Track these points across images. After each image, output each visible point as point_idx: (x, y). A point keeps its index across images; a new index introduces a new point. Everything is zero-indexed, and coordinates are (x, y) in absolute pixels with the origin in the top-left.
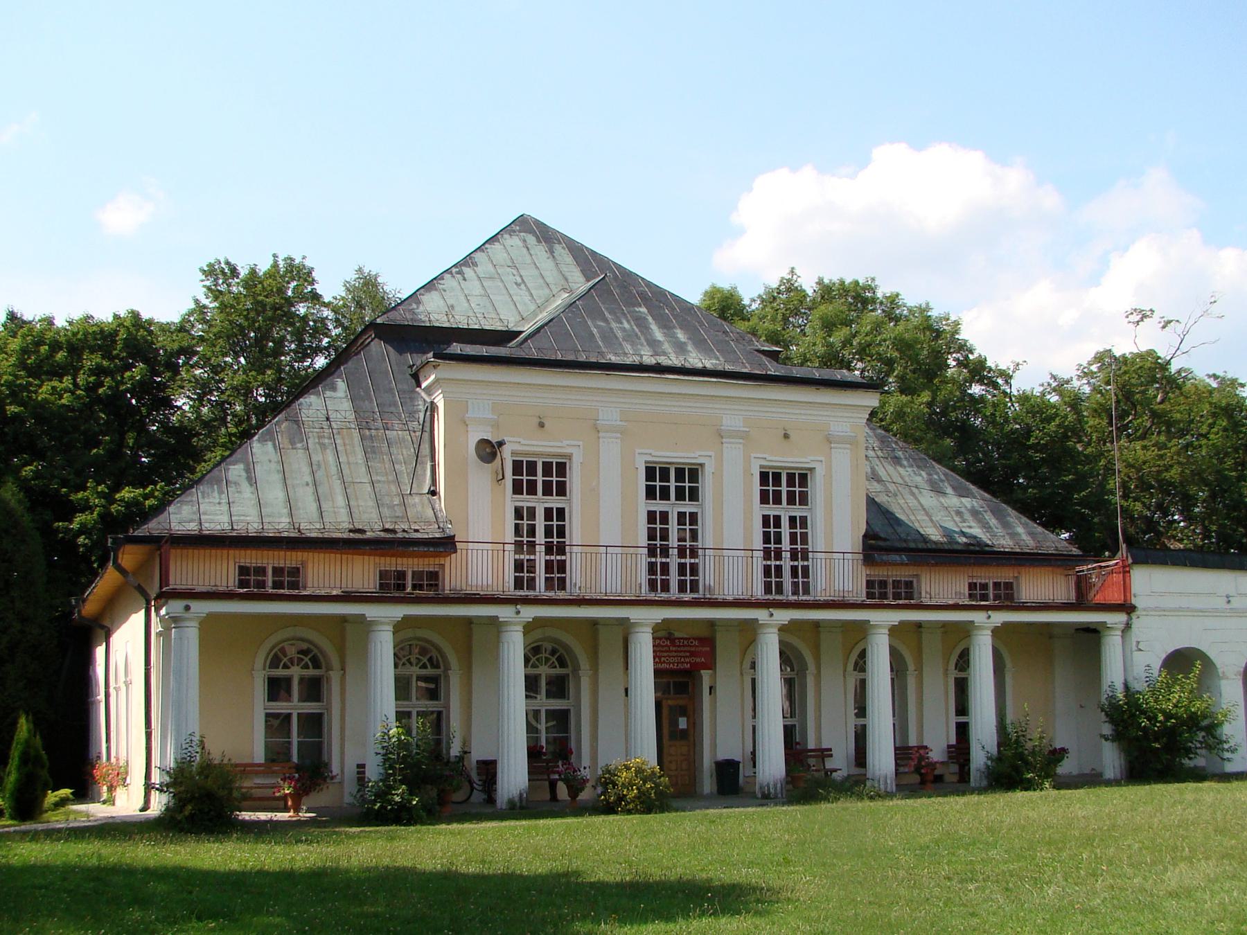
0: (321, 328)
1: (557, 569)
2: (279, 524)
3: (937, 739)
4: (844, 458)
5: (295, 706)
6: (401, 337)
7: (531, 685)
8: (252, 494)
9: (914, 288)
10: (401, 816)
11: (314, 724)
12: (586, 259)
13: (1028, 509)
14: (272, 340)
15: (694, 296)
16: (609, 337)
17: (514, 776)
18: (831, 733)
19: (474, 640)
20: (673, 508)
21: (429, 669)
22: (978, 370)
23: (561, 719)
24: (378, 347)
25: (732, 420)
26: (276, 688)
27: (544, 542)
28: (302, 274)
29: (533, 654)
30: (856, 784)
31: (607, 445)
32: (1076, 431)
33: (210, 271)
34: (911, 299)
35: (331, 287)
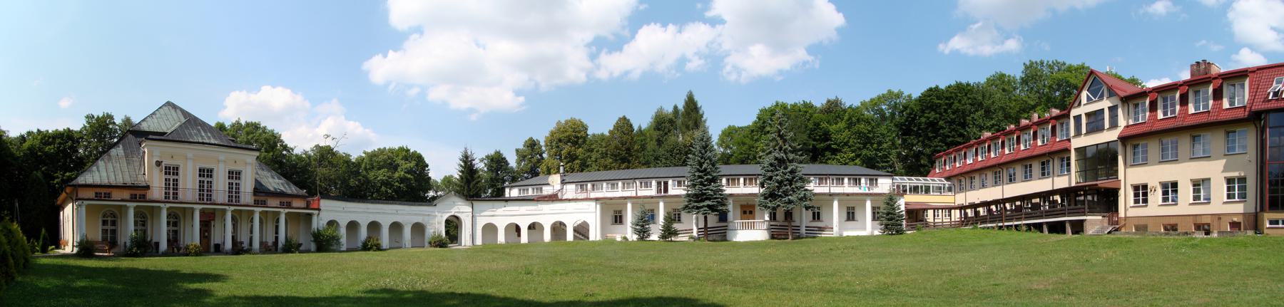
0: (116, 131)
1: (175, 194)
2: (105, 182)
3: (270, 240)
4: (249, 167)
5: (109, 227)
6: (136, 134)
7: (168, 223)
8: (99, 174)
9: (270, 125)
10: (135, 255)
11: (114, 232)
12: (183, 112)
13: (296, 184)
14: (104, 134)
15: (213, 124)
16: (190, 135)
17: (164, 246)
18: (244, 238)
19: (154, 212)
20: (206, 179)
21: (143, 218)
22: (285, 147)
23: (176, 232)
24: (130, 136)
25: (222, 157)
26: (105, 223)
27: (172, 187)
28: (111, 117)
29: (169, 216)
30: (249, 251)
31: (189, 162)
32: (309, 164)
33: (87, 117)
34: (269, 128)
35: (118, 120)
